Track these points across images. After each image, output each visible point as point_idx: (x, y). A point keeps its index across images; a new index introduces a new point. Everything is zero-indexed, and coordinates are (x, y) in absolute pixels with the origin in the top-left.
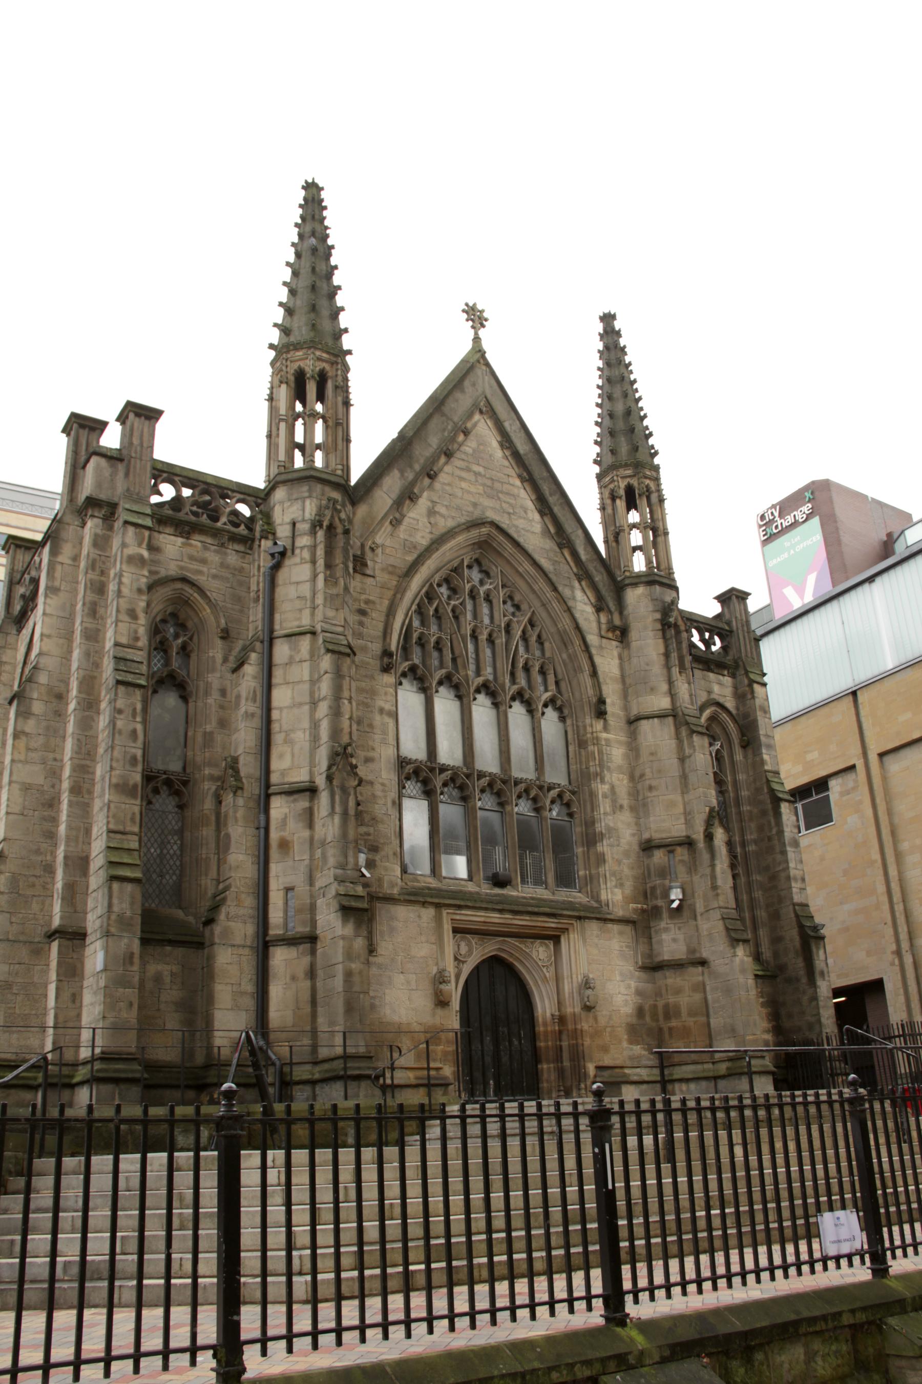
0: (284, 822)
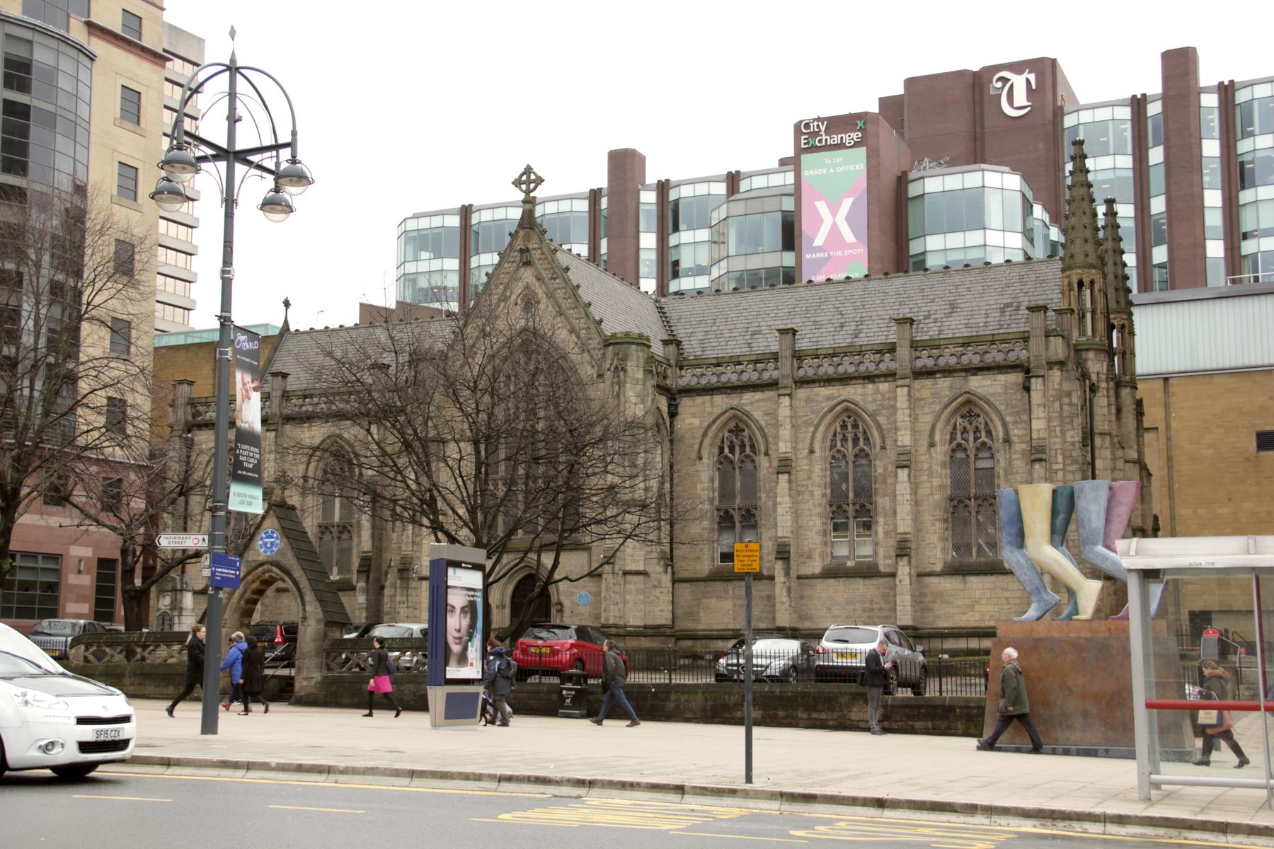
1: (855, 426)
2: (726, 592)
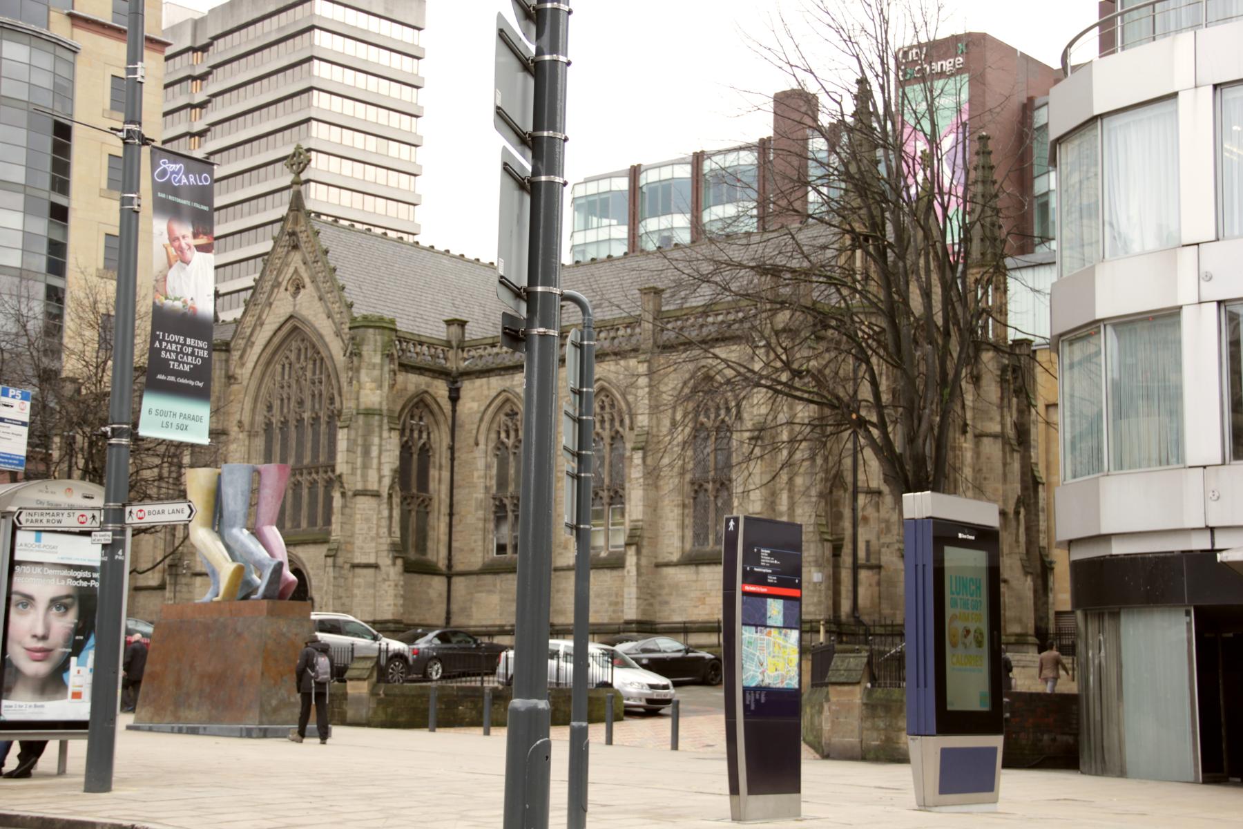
0: (864, 509)
1: (612, 406)
2: (495, 586)
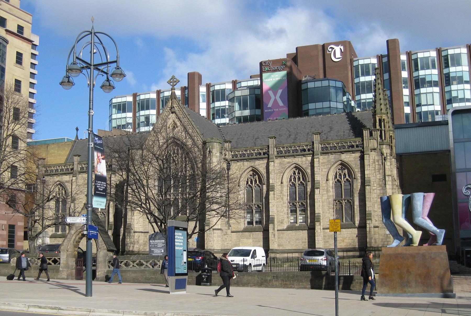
2: (250, 236)
